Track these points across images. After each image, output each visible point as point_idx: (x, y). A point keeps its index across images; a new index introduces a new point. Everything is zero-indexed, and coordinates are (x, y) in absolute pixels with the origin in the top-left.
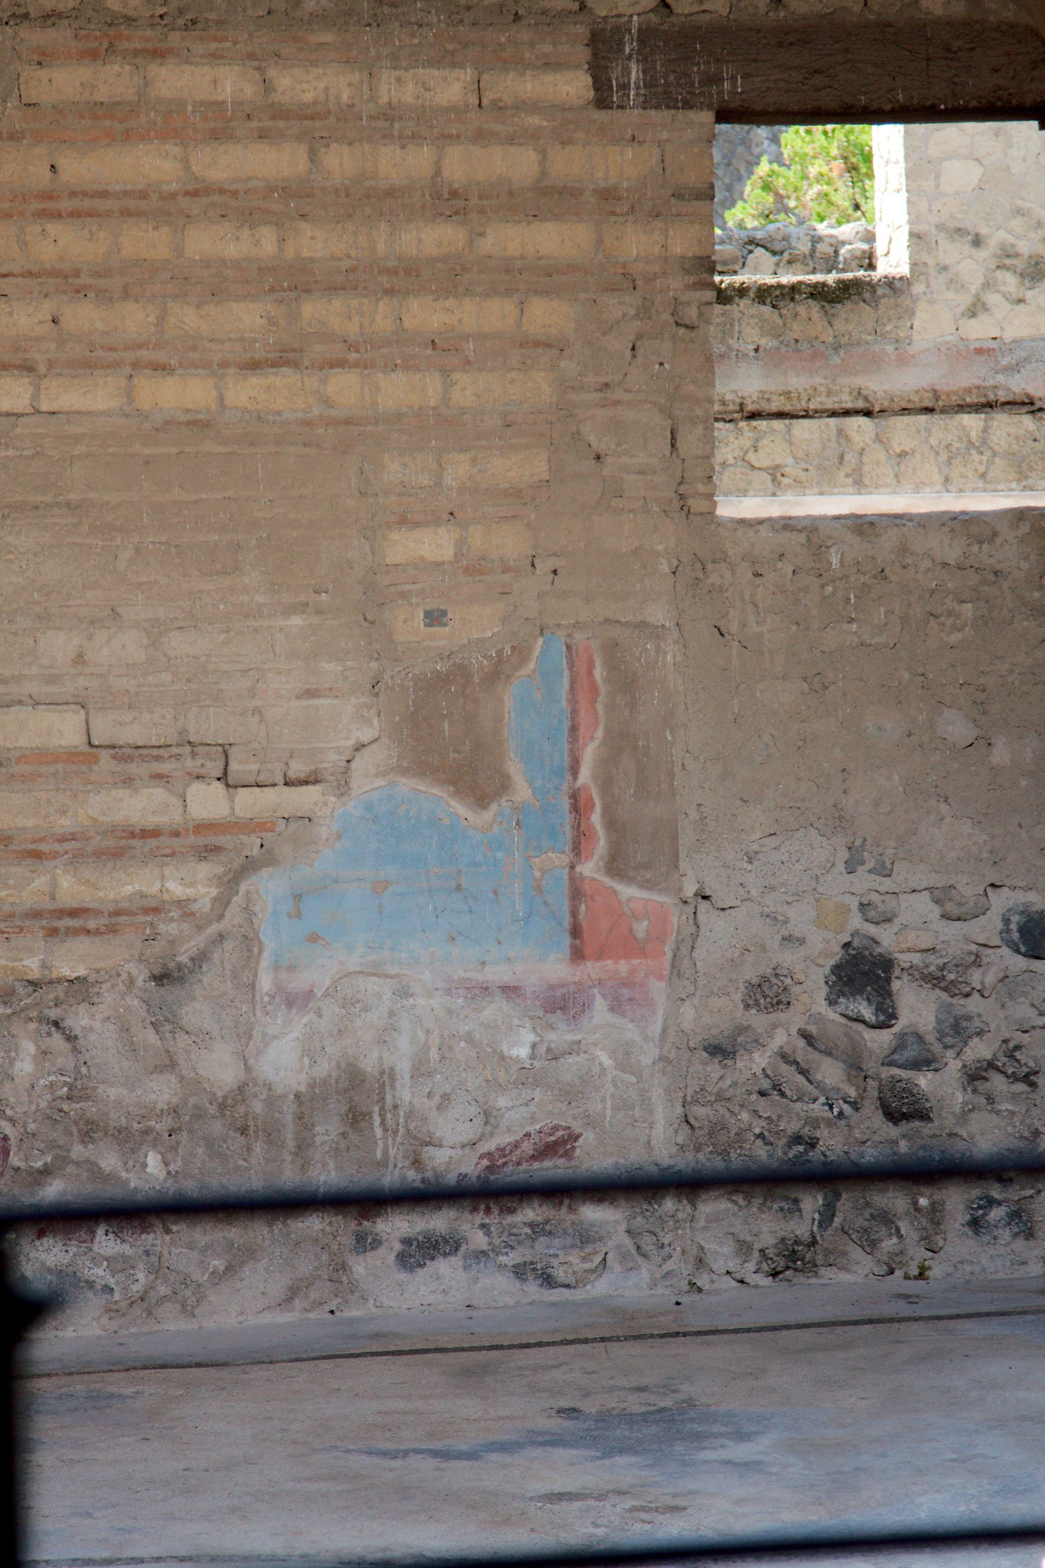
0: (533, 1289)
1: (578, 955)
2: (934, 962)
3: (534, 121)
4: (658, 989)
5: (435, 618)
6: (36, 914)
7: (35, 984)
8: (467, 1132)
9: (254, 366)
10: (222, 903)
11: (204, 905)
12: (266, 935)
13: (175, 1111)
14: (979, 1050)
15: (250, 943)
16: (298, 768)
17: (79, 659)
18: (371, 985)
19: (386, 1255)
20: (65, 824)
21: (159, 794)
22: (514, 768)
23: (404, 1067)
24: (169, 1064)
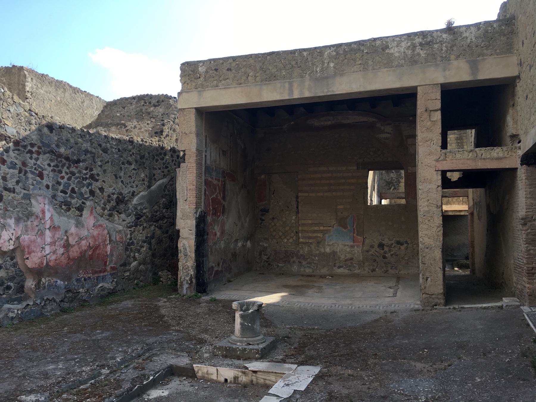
0: (349, 271)
1: (354, 242)
2: (388, 244)
3: (351, 171)
4: (361, 246)
5: (342, 213)
6: (307, 237)
7: (308, 243)
8: (344, 257)
9: (326, 192)
10: (323, 236)
11: (321, 237)
12: (326, 239)
13: (319, 254)
14: (392, 253)
15: (325, 240)
16: (329, 226)
17: (311, 216)
18: (336, 244)
19: (336, 268)
20: (310, 230)
21: (318, 227)
22: (348, 226)
23: (338, 251)
24: (318, 250)
